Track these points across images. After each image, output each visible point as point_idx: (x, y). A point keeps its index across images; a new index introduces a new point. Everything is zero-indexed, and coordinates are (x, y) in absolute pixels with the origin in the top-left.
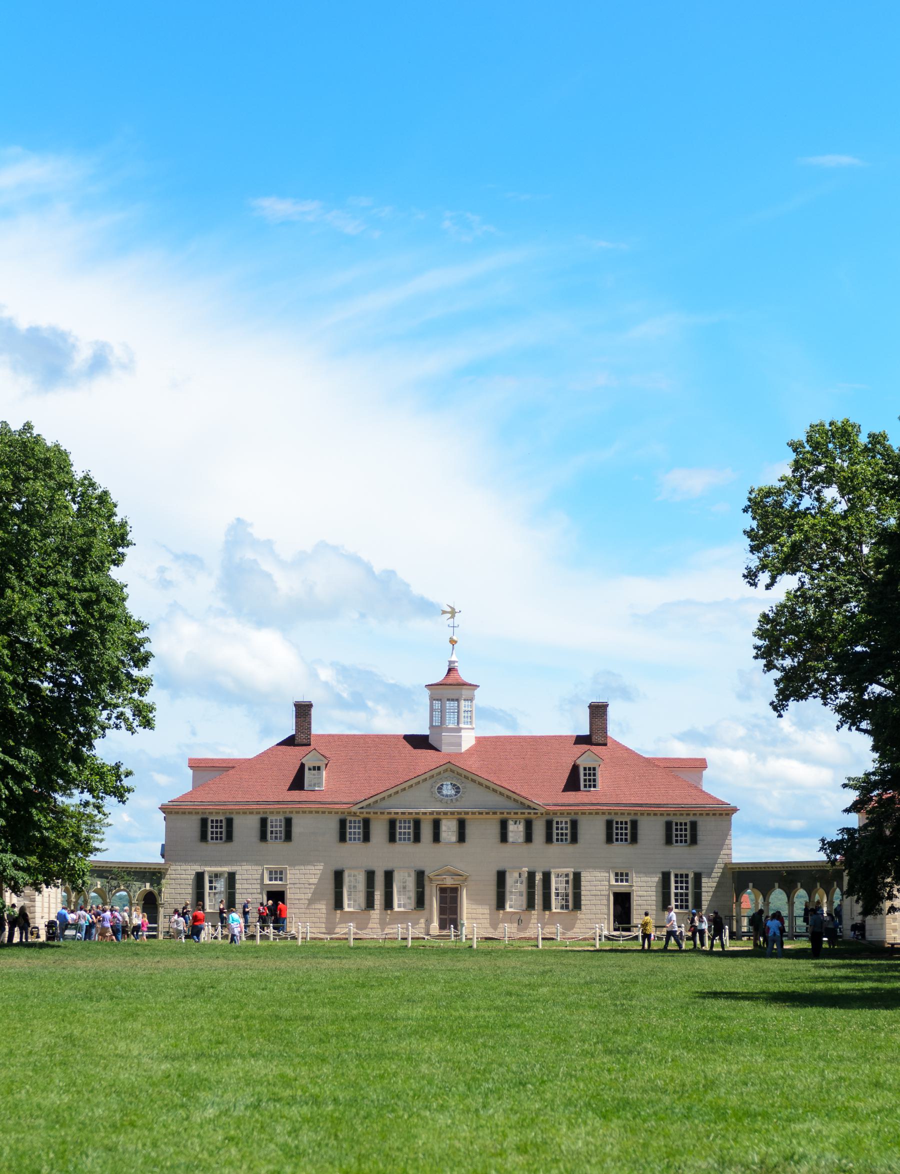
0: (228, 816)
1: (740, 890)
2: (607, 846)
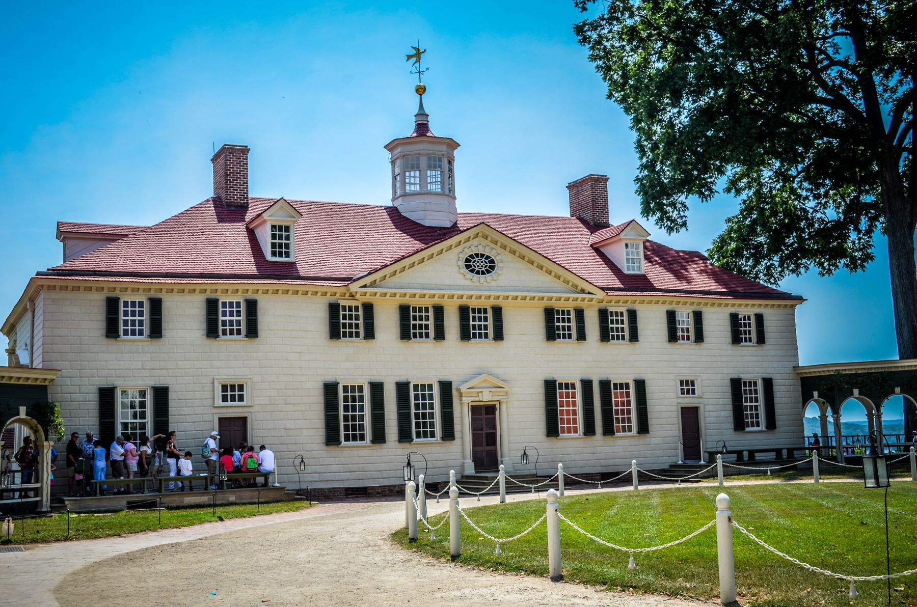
0: (153, 294)
1: (806, 398)
2: (105, 341)
